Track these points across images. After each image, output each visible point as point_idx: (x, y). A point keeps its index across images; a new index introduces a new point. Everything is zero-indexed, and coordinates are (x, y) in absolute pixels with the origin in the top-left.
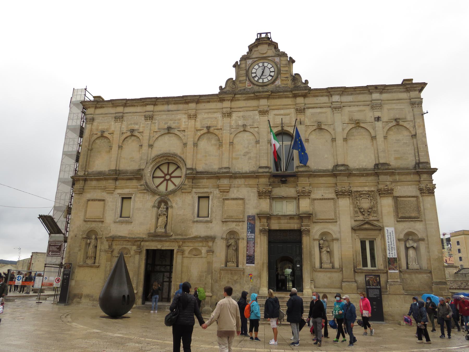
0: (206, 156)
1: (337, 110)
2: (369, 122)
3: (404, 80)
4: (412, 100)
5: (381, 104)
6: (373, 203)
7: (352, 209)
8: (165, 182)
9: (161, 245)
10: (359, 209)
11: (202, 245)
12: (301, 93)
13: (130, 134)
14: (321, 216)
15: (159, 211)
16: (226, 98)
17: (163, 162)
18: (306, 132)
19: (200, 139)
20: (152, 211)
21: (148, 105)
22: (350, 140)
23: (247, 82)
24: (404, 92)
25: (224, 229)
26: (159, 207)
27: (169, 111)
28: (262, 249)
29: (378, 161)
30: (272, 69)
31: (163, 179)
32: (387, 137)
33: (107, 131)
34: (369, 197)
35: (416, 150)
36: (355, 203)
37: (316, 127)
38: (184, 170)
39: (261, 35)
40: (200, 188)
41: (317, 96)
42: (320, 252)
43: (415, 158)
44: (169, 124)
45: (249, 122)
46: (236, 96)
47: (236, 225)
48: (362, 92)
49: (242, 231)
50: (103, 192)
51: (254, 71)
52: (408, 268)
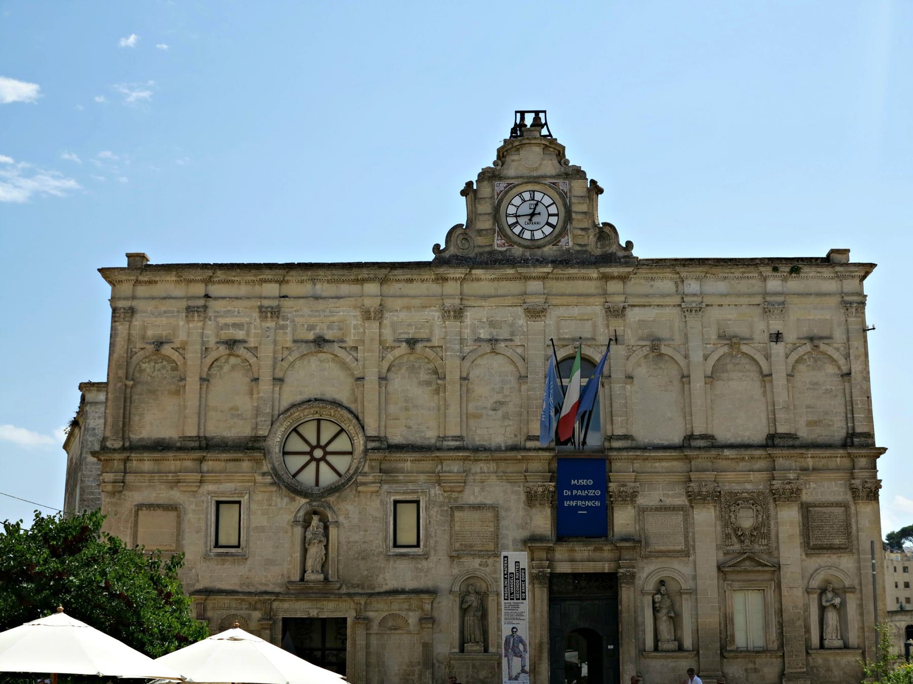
0: (407, 409)
2: (759, 343)
3: (833, 251)
4: (846, 298)
5: (783, 303)
6: (763, 516)
7: (719, 528)
8: (313, 464)
9: (318, 608)
10: (736, 530)
11: (407, 607)
12: (618, 272)
14: (657, 545)
15: (307, 533)
16: (452, 276)
17: (307, 419)
18: (627, 359)
19: (393, 369)
20: (292, 533)
21: (266, 281)
22: (718, 380)
23: (496, 235)
24: (832, 278)
25: (455, 571)
26: (306, 524)
27: (317, 298)
28: (538, 614)
29: (774, 429)
30: (552, 209)
31: (307, 458)
32: (793, 376)
33: (167, 343)
34: (753, 505)
35: (848, 408)
36: (727, 518)
37: (648, 349)
38: (360, 442)
39: (522, 118)
40: (397, 482)
41: (653, 279)
42: (655, 619)
43: (847, 424)
44: (317, 331)
45: (504, 333)
46: (474, 271)
47: (480, 565)
48: (746, 275)
49: (494, 576)
50: (172, 488)
51: (511, 210)
52: (822, 646)
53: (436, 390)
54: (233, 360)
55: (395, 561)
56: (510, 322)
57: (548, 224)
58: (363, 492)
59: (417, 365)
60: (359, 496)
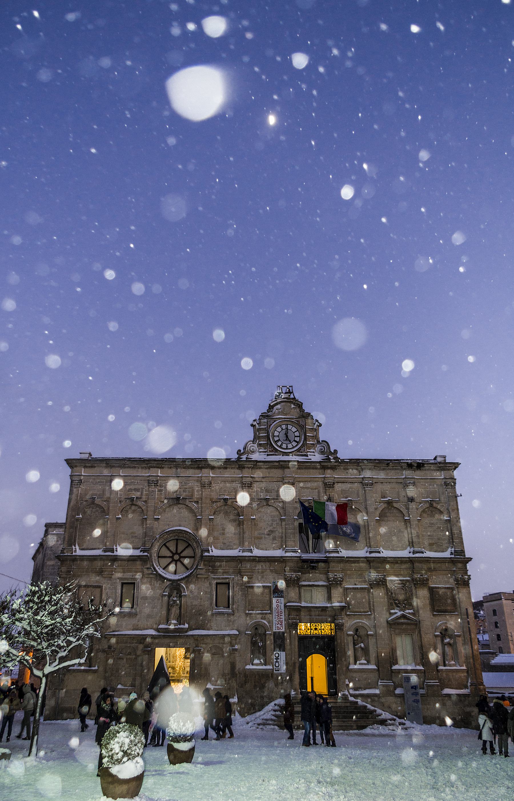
1: (369, 486)
13: (131, 503)
17: (171, 539)
20: (162, 600)
21: (152, 467)
24: (438, 470)
30: (297, 434)
46: (258, 464)
48: (394, 468)
53: (238, 524)
54: (133, 508)
55: (216, 616)
56: (276, 489)
57: (295, 441)
58: (200, 578)
59: (228, 511)
60: (198, 580)
